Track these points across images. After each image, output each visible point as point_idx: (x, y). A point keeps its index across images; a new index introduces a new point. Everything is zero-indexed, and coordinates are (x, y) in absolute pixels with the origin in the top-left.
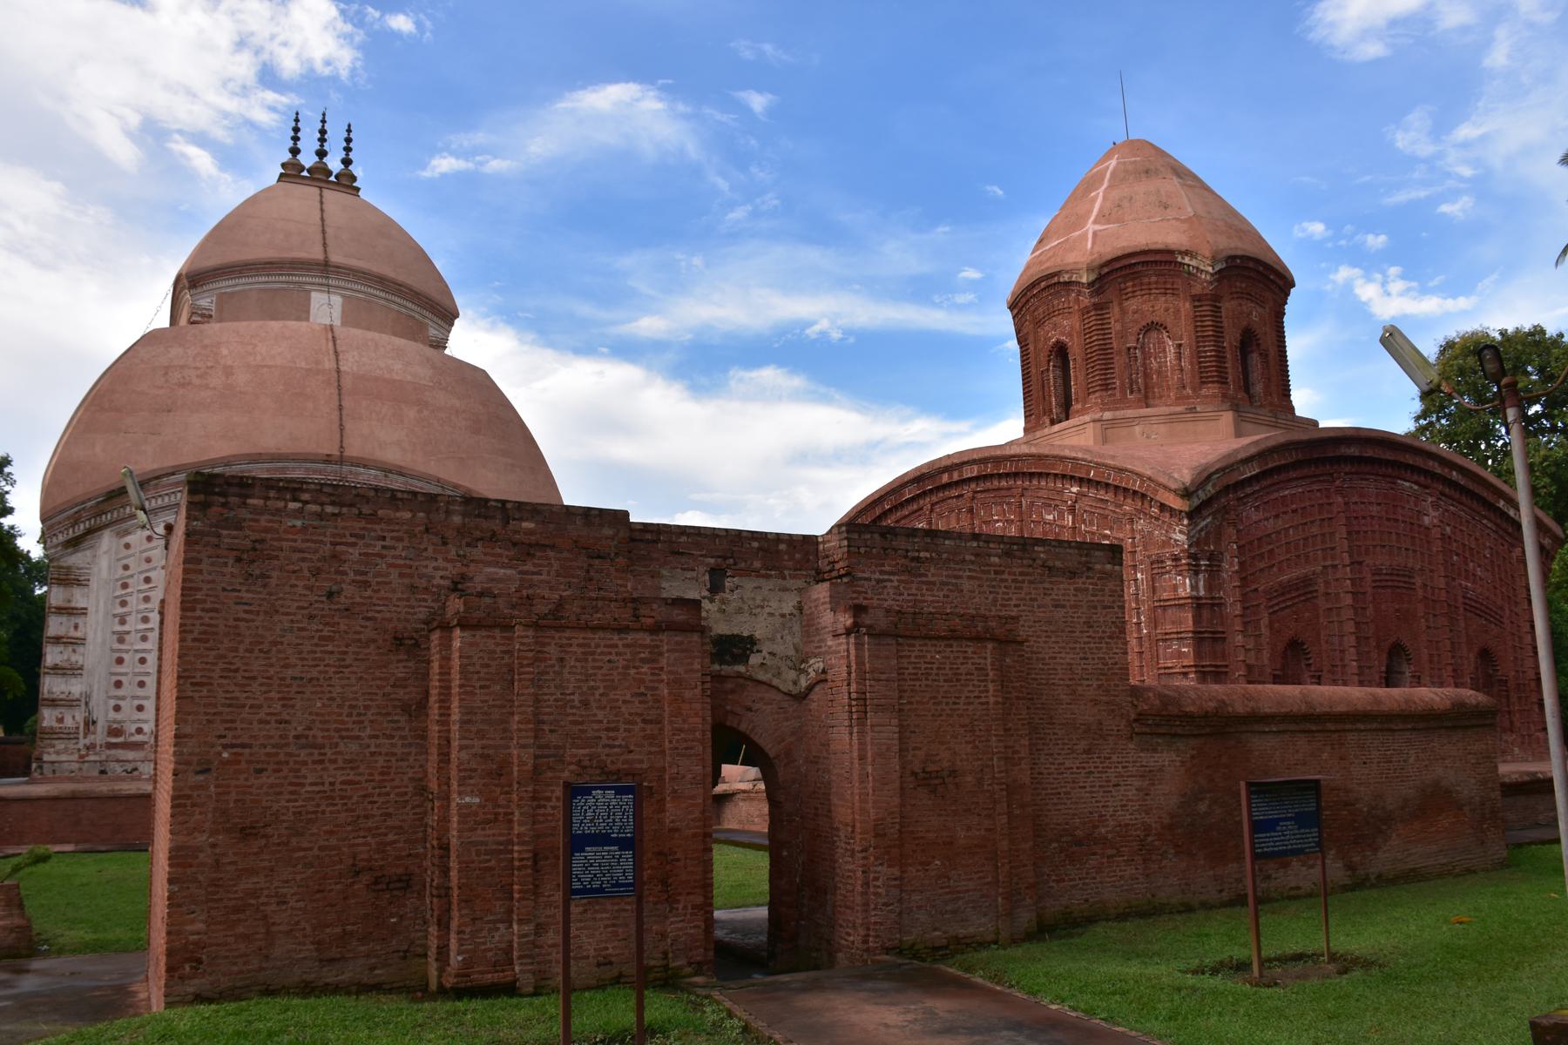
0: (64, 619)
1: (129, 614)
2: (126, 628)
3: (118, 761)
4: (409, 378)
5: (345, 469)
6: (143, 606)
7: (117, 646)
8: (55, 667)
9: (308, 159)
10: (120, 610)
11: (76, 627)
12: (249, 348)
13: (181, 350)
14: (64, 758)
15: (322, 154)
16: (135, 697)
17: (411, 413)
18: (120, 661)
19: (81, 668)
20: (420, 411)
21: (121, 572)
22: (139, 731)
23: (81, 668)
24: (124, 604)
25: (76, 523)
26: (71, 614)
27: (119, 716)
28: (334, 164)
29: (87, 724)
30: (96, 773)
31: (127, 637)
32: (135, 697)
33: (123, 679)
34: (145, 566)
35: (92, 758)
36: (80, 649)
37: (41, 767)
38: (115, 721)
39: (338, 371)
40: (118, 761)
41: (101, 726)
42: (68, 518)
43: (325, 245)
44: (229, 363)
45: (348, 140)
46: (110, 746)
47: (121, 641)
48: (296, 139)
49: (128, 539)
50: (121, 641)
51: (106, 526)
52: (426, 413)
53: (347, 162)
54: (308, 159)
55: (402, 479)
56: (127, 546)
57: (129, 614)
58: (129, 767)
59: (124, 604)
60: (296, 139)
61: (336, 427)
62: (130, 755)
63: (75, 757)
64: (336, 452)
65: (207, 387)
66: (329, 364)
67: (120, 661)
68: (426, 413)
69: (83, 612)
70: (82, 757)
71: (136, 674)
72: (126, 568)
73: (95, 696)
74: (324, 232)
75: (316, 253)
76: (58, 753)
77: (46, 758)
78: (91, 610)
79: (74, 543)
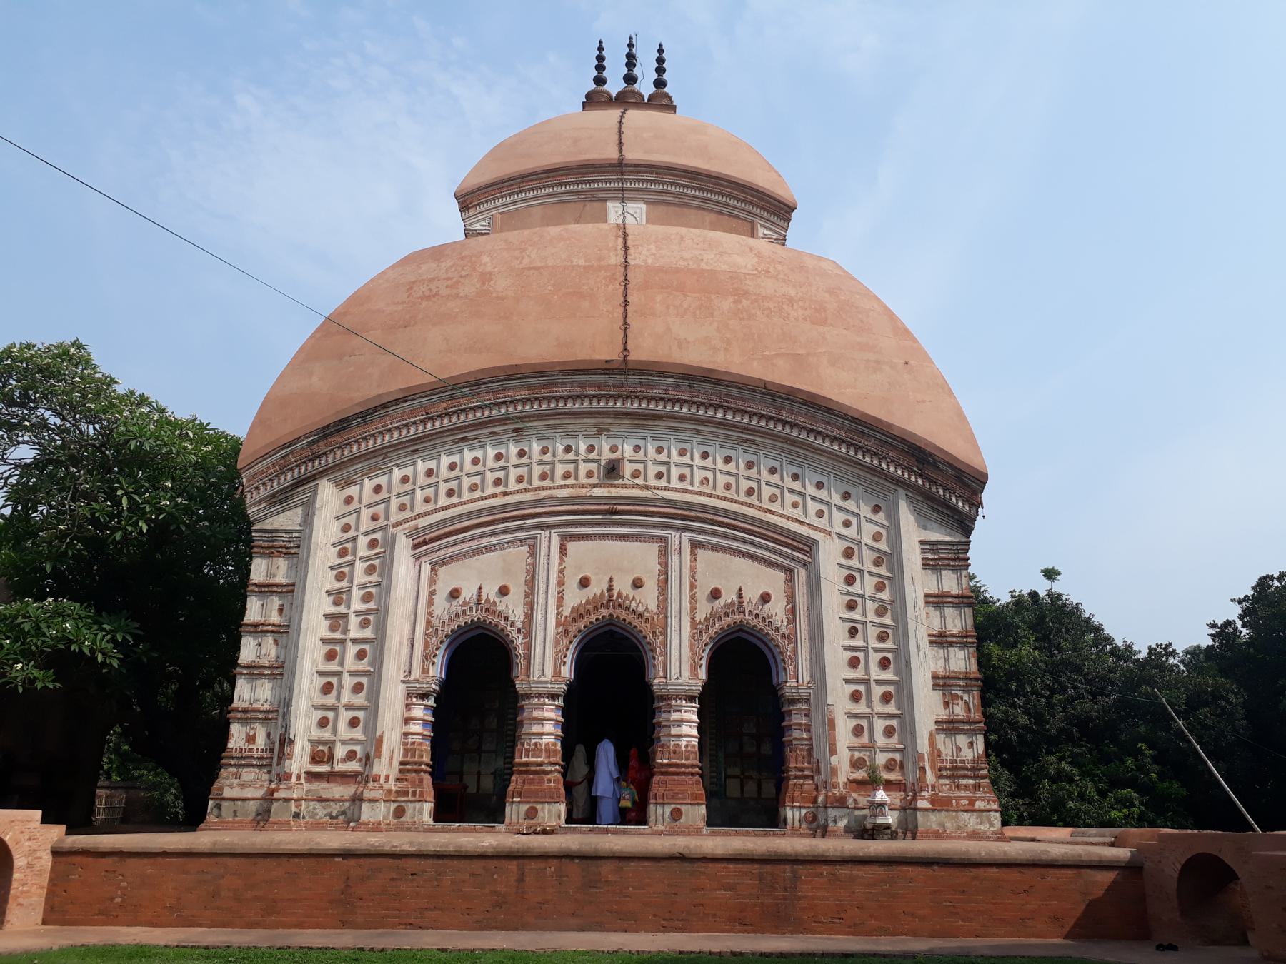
3: (320, 800)
4: (725, 267)
5: (633, 379)
9: (615, 85)
12: (517, 253)
13: (434, 265)
14: (249, 793)
15: (630, 79)
17: (727, 304)
27: (326, 734)
37: (219, 807)
38: (320, 742)
43: (620, 144)
44: (489, 269)
45: (660, 61)
46: (312, 776)
48: (600, 68)
49: (353, 490)
52: (745, 303)
53: (660, 83)
54: (615, 85)
60: (600, 68)
65: (457, 296)
66: (615, 259)
68: (745, 303)
74: (620, 132)
75: (612, 154)
76: (242, 786)
77: (227, 793)
79: (280, 499)
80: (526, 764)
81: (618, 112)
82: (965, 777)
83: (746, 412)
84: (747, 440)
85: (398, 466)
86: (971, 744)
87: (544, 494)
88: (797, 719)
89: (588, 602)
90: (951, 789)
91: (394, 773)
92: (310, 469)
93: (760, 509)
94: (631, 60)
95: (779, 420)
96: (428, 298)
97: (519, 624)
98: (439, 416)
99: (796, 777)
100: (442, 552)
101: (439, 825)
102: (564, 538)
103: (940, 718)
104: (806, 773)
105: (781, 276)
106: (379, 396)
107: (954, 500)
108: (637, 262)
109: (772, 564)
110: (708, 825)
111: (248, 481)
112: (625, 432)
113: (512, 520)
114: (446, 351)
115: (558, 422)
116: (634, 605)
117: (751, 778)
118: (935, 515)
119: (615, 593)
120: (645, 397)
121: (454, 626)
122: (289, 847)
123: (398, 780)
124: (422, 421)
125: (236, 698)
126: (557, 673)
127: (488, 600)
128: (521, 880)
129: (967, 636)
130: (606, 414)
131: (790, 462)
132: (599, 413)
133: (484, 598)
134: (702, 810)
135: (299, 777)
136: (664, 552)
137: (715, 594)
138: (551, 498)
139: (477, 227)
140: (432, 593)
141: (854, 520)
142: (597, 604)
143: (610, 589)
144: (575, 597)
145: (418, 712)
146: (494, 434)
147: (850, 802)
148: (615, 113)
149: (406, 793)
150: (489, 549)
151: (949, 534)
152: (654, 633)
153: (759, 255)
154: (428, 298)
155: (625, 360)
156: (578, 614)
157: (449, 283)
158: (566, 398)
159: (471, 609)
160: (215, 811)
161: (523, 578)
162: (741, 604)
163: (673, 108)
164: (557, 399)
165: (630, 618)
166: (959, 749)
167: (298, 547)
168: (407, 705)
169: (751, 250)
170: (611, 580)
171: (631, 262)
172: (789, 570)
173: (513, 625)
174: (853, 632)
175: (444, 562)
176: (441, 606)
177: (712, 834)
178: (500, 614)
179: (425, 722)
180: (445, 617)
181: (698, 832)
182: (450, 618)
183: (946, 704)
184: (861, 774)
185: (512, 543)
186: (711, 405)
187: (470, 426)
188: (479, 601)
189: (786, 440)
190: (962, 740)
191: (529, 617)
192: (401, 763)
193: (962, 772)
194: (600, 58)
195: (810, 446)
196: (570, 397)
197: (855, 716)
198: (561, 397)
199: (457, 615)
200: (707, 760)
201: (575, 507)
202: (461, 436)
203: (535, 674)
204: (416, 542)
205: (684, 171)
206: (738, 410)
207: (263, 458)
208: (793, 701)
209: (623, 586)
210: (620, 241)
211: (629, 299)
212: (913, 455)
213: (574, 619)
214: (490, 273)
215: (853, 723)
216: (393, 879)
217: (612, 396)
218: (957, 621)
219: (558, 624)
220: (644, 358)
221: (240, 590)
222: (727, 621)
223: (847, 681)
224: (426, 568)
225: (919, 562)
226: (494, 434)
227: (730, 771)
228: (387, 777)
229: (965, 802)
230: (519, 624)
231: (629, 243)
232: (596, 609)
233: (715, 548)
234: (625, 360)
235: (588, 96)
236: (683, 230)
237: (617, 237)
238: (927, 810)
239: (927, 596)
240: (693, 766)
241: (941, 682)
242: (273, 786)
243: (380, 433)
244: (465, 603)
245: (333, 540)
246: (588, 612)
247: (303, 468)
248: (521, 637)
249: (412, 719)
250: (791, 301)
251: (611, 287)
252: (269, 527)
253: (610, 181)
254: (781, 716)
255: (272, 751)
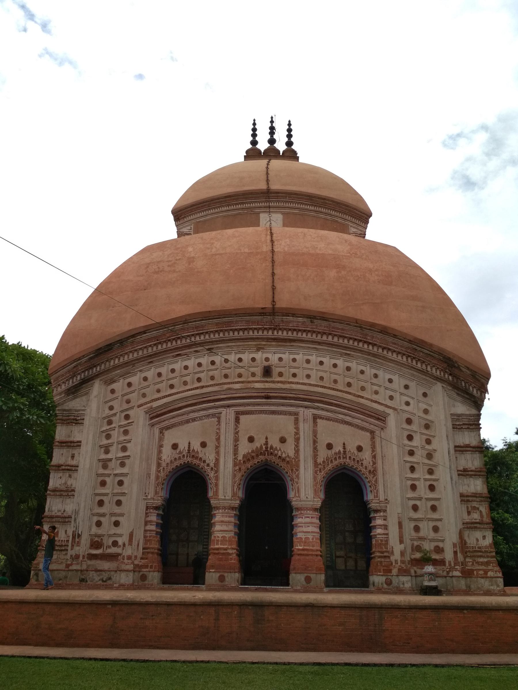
0: (64, 451)
1: (111, 445)
2: (109, 456)
3: (97, 571)
4: (330, 252)
5: (278, 319)
6: (122, 438)
7: (101, 471)
8: (54, 491)
9: (263, 145)
10: (105, 442)
11: (73, 457)
12: (208, 246)
13: (161, 253)
15: (272, 141)
16: (112, 514)
18: (103, 484)
19: (73, 491)
20: (337, 272)
21: (107, 412)
22: (115, 544)
23: (73, 491)
24: (108, 437)
25: (74, 376)
26: (69, 446)
27: (100, 531)
28: (281, 146)
29: (74, 537)
30: (76, 581)
31: (109, 464)
32: (112, 514)
33: (104, 498)
34: (125, 406)
35: (74, 567)
36: (74, 475)
38: (96, 535)
39: (273, 251)
40: (97, 571)
41: (85, 540)
42: (69, 371)
43: (268, 181)
44: (192, 255)
45: (289, 130)
47: (105, 467)
48: (254, 135)
49: (114, 386)
50: (105, 467)
51: (97, 376)
52: (343, 273)
53: (289, 144)
54: (263, 145)
55: (325, 323)
56: (113, 391)
57: (111, 445)
58: (105, 576)
59: (108, 437)
60: (254, 135)
61: (269, 288)
62: (106, 565)
63: (63, 567)
64: (269, 305)
65: (174, 271)
66: (266, 248)
67: (103, 484)
69: (78, 444)
70: (68, 566)
71: (114, 495)
72: (111, 408)
73: (81, 514)
74: (267, 174)
75: (263, 186)
78: (83, 443)
79: (74, 391)
80: (218, 549)
81: (265, 161)
82: (481, 556)
83: (346, 337)
84: (346, 354)
85: (141, 371)
86: (484, 537)
87: (226, 387)
88: (379, 522)
89: (253, 451)
90: (473, 564)
91: (140, 554)
92: (90, 373)
93: (354, 395)
94: (272, 130)
95: (365, 342)
96: (156, 273)
97: (212, 465)
98: (165, 342)
99: (380, 557)
100: (167, 422)
101: (166, 586)
102: (238, 415)
103: (465, 521)
104: (385, 554)
105: (364, 257)
106: (130, 330)
107: (471, 388)
108: (279, 249)
109: (363, 429)
110: (327, 586)
111: (54, 381)
112: (273, 349)
113: (206, 402)
114: (169, 304)
115: (234, 344)
116: (280, 453)
117: (351, 557)
118: (459, 398)
119: (269, 447)
120: (285, 329)
121: (174, 466)
122: (80, 599)
123: (142, 558)
124: (155, 345)
125: (47, 509)
126: (234, 495)
127: (193, 450)
128: (217, 619)
129: (480, 471)
130: (262, 339)
131: (372, 367)
132: (258, 338)
133: (191, 449)
134: (323, 577)
135: (84, 556)
136: (297, 421)
137: (329, 446)
138: (230, 389)
139: (185, 230)
140: (161, 446)
141: (411, 402)
142: (258, 452)
143: (266, 443)
144: (245, 448)
145: (153, 518)
146: (196, 351)
147: (412, 571)
148: (263, 162)
149: (147, 567)
150: (194, 420)
151: (468, 410)
152: (292, 470)
153: (350, 244)
154: (156, 273)
155: (273, 308)
156: (247, 458)
157: (170, 263)
158: (238, 330)
159: (184, 455)
160: (35, 577)
161: (214, 438)
162: (345, 452)
163: (297, 159)
164: (234, 331)
165: (277, 461)
166: (477, 540)
167: (83, 419)
168: (146, 514)
169: (346, 241)
170: (267, 438)
171: (276, 250)
172: (372, 432)
173: (208, 465)
174: (412, 469)
175: (168, 428)
176: (167, 453)
177: (330, 592)
178: (201, 459)
179: (157, 525)
180: (169, 461)
181: (321, 592)
182: (171, 461)
183: (469, 513)
184: (418, 555)
185: (208, 416)
186: (325, 333)
187: (182, 347)
188: (189, 450)
189: (369, 354)
190: (478, 534)
191: (217, 460)
192: (144, 549)
193: (480, 554)
194: (254, 130)
195: (383, 357)
196: (241, 329)
197: (415, 520)
198: (236, 330)
199: (175, 459)
200: (324, 546)
201: (244, 395)
202: (178, 353)
203: (221, 496)
204: (151, 416)
205: (305, 196)
206: (341, 336)
207: (64, 367)
208: (377, 511)
209: (274, 442)
210: (269, 237)
211: (275, 272)
212: (446, 362)
213: (244, 462)
214: (193, 257)
215: (412, 524)
216: (141, 618)
217: (266, 329)
218: (474, 462)
219: (235, 465)
220: (284, 305)
221: (49, 443)
222: (335, 463)
223: (409, 499)
224: (157, 431)
225: (451, 427)
226: (196, 351)
227: (338, 554)
228: (136, 557)
229: (481, 572)
230: (212, 465)
231: (274, 238)
232: (257, 456)
233: (328, 419)
234: (273, 308)
235: (247, 152)
236: (306, 230)
237: (266, 235)
238: (458, 577)
239: (456, 447)
240: (317, 550)
241: (465, 499)
242: (69, 562)
243: (131, 352)
244: (180, 453)
245: (104, 416)
246: (253, 457)
247: (86, 373)
248: (213, 472)
249: (151, 521)
250: (370, 271)
251: (264, 265)
252: (67, 408)
253: (262, 202)
254: (369, 520)
255: (68, 541)
